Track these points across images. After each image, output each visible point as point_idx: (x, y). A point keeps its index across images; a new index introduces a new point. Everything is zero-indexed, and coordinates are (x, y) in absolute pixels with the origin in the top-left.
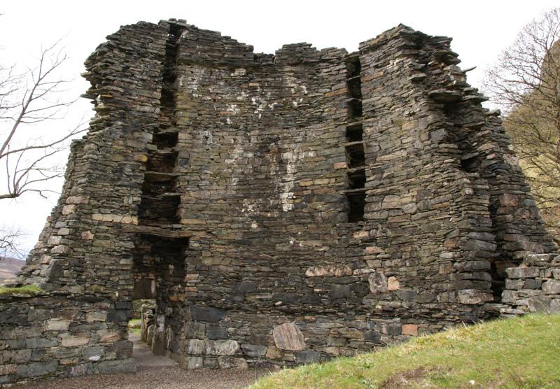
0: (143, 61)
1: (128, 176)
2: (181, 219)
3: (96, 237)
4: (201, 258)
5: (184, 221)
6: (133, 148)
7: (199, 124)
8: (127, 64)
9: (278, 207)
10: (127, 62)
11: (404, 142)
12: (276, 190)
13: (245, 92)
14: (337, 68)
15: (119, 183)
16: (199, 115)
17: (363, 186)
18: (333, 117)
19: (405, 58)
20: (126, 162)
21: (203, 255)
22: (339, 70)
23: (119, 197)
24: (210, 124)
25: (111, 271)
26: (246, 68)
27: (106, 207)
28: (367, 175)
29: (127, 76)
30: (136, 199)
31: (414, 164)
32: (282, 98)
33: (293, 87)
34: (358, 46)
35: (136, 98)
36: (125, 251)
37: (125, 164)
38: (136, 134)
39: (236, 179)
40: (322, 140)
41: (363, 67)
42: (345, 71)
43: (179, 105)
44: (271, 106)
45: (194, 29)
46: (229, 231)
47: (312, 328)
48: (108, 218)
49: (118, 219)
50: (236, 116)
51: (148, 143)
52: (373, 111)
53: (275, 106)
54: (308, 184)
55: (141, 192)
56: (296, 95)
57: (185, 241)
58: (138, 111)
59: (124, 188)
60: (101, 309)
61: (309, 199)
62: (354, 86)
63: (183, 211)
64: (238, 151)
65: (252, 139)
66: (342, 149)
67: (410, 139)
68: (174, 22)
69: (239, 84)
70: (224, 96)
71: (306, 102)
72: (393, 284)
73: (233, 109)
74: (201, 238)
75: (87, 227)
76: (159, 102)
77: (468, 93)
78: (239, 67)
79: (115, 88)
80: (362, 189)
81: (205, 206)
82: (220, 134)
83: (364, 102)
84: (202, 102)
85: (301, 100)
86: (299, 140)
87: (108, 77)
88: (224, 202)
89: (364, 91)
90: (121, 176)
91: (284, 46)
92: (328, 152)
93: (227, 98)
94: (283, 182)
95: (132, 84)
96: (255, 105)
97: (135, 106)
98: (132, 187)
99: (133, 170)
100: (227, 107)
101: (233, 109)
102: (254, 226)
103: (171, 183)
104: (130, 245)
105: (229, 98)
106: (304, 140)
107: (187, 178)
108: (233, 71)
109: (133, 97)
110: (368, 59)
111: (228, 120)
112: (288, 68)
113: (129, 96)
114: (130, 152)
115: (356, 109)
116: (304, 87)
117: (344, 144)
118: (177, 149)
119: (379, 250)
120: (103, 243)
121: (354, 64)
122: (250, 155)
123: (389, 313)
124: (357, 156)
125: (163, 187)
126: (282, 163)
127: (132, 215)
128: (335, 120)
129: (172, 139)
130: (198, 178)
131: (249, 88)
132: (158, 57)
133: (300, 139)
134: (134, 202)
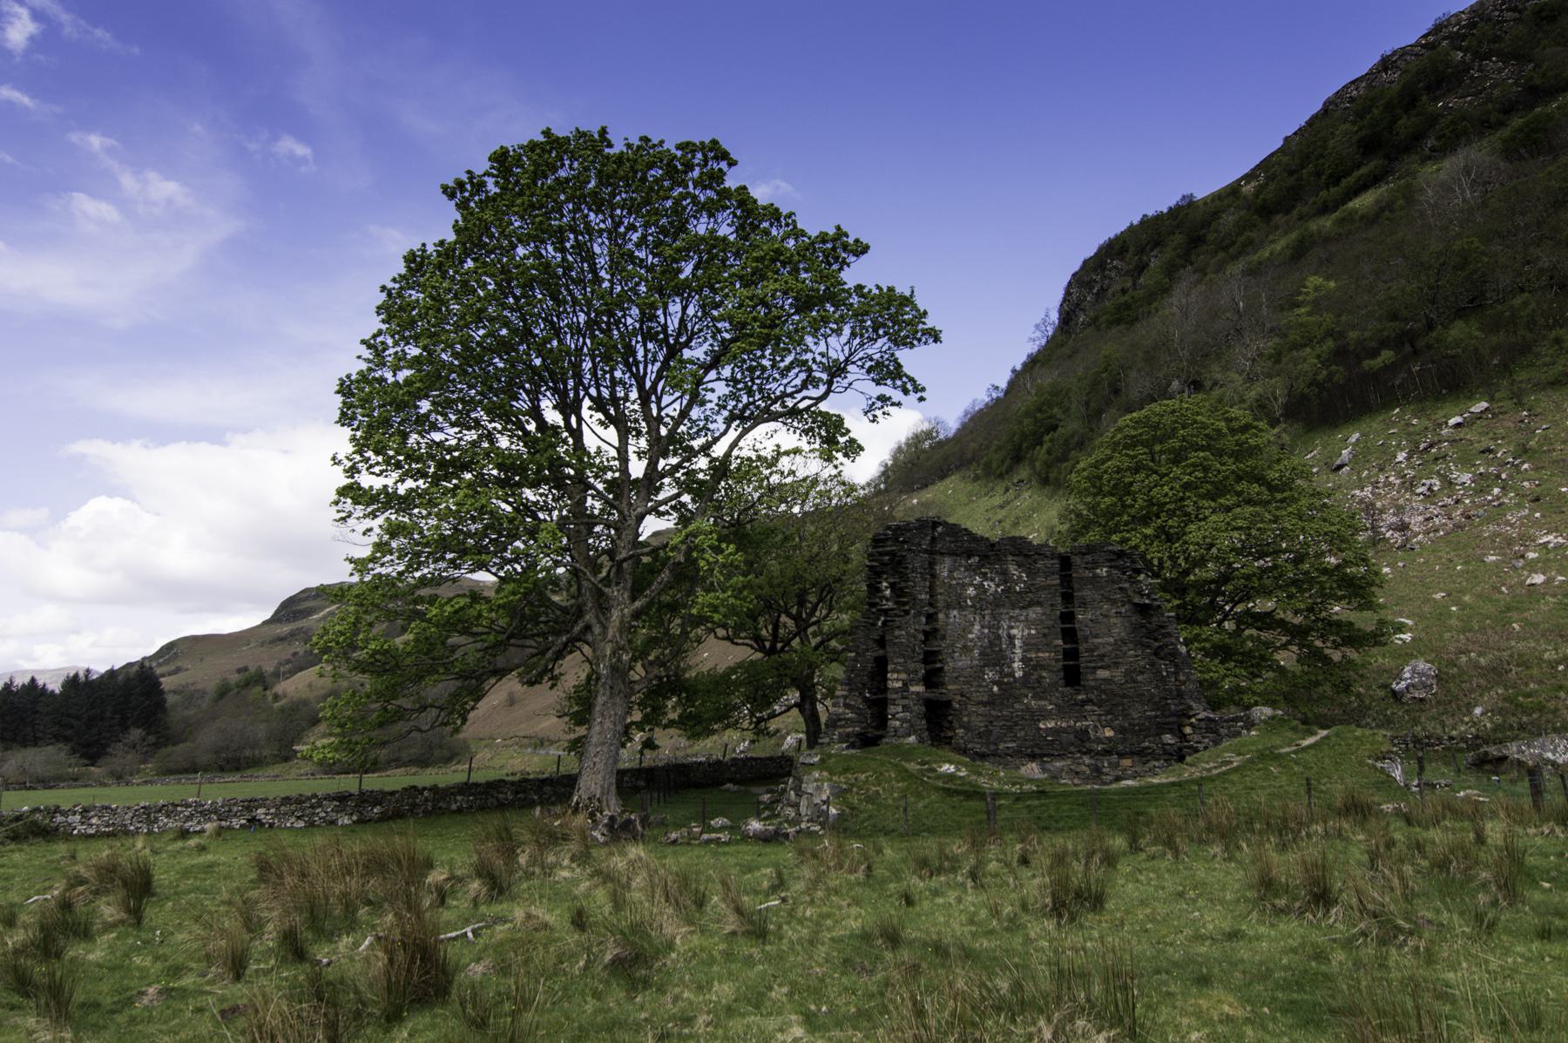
9: (1012, 674)
47: (1048, 766)
57: (948, 704)
61: (1035, 668)
62: (1066, 580)
64: (977, 627)
69: (974, 570)
72: (1109, 733)
84: (950, 586)
89: (1076, 586)
101: (971, 591)
102: (995, 689)
106: (1027, 620)
110: (1077, 560)
115: (1068, 598)
117: (1060, 626)
121: (1065, 562)
123: (1107, 752)
124: (1070, 635)
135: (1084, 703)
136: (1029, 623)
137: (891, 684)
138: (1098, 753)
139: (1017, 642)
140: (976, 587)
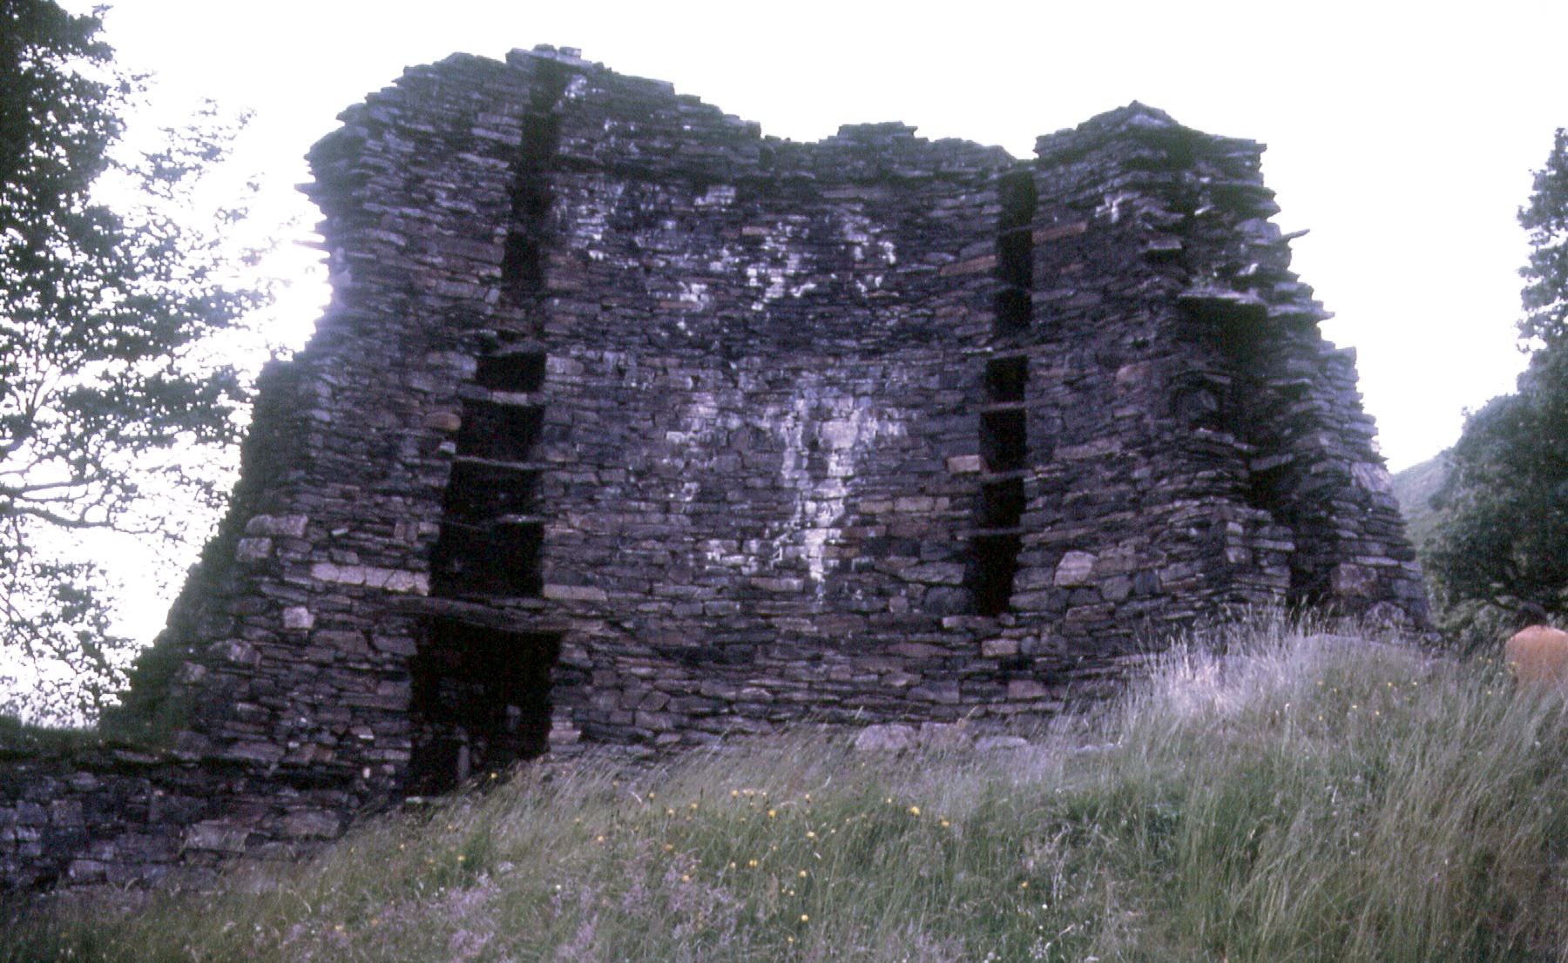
0: (461, 160)
1: (410, 468)
2: (541, 584)
3: (320, 624)
4: (588, 689)
5: (552, 591)
6: (426, 394)
7: (604, 333)
8: (415, 170)
10: (417, 163)
11: (1119, 414)
12: (797, 518)
13: (731, 249)
14: (978, 198)
15: (385, 485)
16: (605, 309)
17: (1017, 524)
18: (958, 332)
19: (1137, 195)
20: (406, 431)
21: (596, 683)
22: (981, 206)
23: (384, 521)
24: (632, 333)
25: (353, 710)
26: (735, 183)
27: (346, 548)
28: (1028, 496)
29: (415, 204)
30: (425, 527)
31: (1136, 475)
32: (828, 271)
33: (859, 244)
34: (1033, 143)
35: (438, 260)
36: (391, 662)
37: (400, 437)
38: (434, 358)
39: (694, 486)
40: (922, 391)
41: (1043, 203)
42: (997, 209)
43: (553, 283)
44: (797, 293)
45: (598, 74)
46: (667, 623)
48: (353, 576)
49: (376, 578)
50: (704, 315)
51: (466, 381)
52: (1058, 325)
53: (808, 295)
54: (880, 508)
55: (438, 509)
56: (868, 266)
57: (551, 643)
58: (443, 297)
59: (398, 499)
60: (325, 805)
63: (550, 564)
64: (704, 408)
65: (742, 378)
66: (973, 421)
67: (1130, 411)
68: (546, 55)
70: (673, 259)
71: (890, 285)
73: (695, 294)
74: (593, 638)
75: (295, 596)
76: (497, 272)
77: (1285, 298)
78: (718, 181)
79: (383, 235)
80: (1012, 531)
81: (607, 553)
82: (657, 361)
83: (1035, 298)
85: (878, 280)
86: (864, 388)
87: (367, 206)
88: (658, 546)
89: (1040, 268)
90: (390, 467)
91: (844, 130)
92: (934, 426)
93: (681, 264)
94: (814, 499)
95: (429, 222)
96: (757, 289)
97: (433, 282)
98: (422, 495)
99: (423, 453)
100: (680, 290)
101: (695, 294)
103: (522, 490)
104: (408, 648)
105: (690, 265)
106: (879, 393)
107: (564, 476)
108: (703, 194)
109: (429, 259)
111: (682, 325)
112: (851, 192)
113: (418, 256)
114: (416, 403)
116: (889, 245)
118: (542, 399)
119: (1038, 691)
120: (337, 636)
122: (735, 422)
124: (1006, 440)
125: (502, 496)
127: (414, 571)
128: (963, 341)
129: (529, 372)
130: (593, 479)
131: (743, 240)
132: (501, 150)
133: (868, 385)
134: (422, 537)
139: (837, 467)
140: (715, 283)
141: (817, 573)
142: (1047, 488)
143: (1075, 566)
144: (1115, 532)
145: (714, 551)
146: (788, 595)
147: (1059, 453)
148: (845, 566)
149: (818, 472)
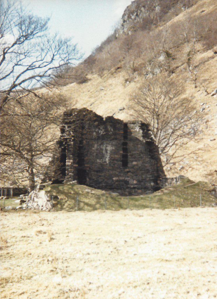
9: (105, 162)
57: (85, 171)
64: (96, 146)
92: (118, 148)
101: (95, 133)
122: (99, 147)
124: (125, 150)
126: (106, 150)
133: (111, 144)
135: (128, 172)
136: (112, 145)
137: (67, 164)
138: (131, 188)
139: (109, 152)
141: (107, 162)
142: (130, 155)
143: (134, 163)
144: (139, 160)
145: (98, 160)
146: (105, 165)
147: (132, 152)
148: (110, 162)
149: (107, 152)
